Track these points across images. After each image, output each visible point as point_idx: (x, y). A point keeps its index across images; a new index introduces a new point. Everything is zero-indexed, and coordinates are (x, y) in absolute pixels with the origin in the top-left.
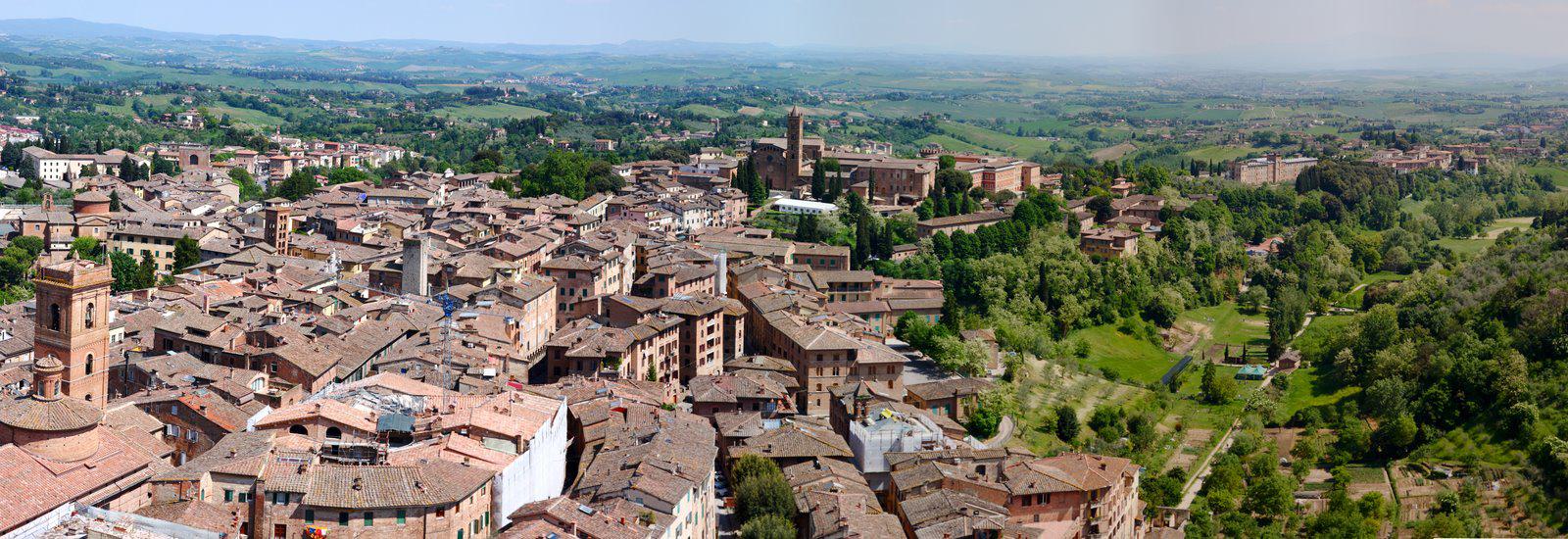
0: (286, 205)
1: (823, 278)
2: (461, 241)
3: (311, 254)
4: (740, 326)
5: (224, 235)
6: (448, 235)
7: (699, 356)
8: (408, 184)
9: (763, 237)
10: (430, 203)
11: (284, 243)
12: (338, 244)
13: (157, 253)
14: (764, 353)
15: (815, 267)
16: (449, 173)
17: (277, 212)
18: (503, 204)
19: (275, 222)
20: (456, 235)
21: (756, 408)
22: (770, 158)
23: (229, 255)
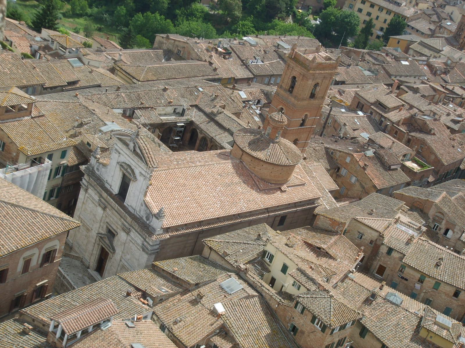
13: (377, 18)
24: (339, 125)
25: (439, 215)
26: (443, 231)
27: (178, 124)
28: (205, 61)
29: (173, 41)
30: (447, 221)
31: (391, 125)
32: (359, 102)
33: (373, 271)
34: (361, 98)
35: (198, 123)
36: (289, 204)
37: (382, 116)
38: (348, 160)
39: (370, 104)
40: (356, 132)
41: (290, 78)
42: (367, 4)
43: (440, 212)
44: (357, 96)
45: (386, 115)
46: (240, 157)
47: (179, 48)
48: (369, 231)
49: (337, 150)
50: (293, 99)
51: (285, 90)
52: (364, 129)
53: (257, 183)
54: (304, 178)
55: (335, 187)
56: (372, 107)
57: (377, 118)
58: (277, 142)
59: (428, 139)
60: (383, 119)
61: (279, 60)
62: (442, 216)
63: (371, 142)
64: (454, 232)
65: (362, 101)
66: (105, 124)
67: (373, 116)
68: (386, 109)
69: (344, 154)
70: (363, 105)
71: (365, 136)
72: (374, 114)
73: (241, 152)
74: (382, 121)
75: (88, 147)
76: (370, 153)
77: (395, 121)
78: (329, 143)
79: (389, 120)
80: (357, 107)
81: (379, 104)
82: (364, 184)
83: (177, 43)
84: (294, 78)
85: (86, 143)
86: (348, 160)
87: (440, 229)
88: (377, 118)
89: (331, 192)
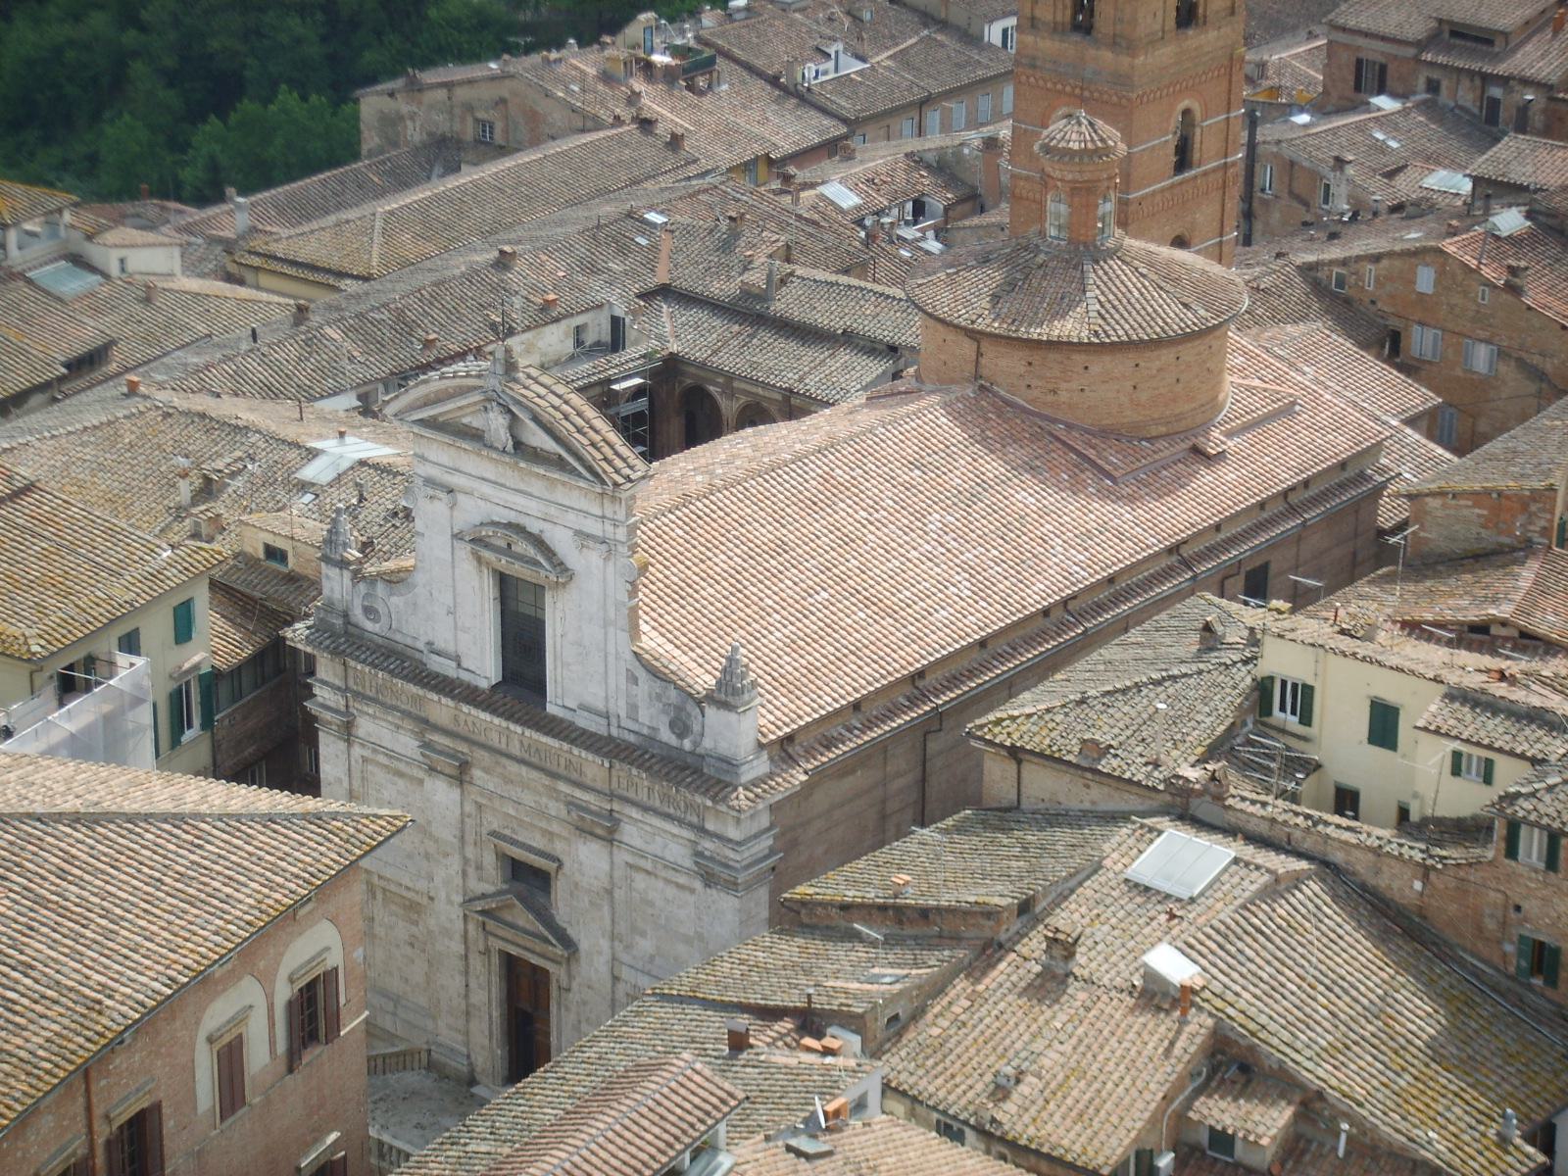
24: (1314, 176)
27: (616, 387)
28: (618, 121)
29: (441, 94)
31: (1542, 103)
32: (1359, 62)
34: (1361, 41)
35: (700, 355)
36: (1262, 505)
37: (1487, 79)
38: (1425, 280)
39: (1411, 52)
40: (1400, 181)
45: (1501, 69)
46: (970, 368)
47: (481, 115)
49: (1359, 258)
52: (1433, 160)
53: (1091, 453)
54: (1279, 380)
55: (1420, 397)
56: (1428, 57)
57: (1467, 96)
58: (1112, 253)
60: (1496, 92)
61: (926, 32)
63: (1491, 191)
65: (1374, 50)
66: (313, 454)
67: (1444, 98)
68: (1490, 42)
69: (1398, 263)
70: (1383, 68)
71: (1451, 182)
72: (1445, 84)
73: (968, 348)
74: (1494, 104)
75: (274, 565)
76: (1510, 220)
77: (1554, 79)
78: (1306, 250)
79: (1527, 82)
80: (1358, 88)
81: (1454, 34)
82: (1536, 360)
83: (462, 94)
85: (261, 554)
88: (1467, 96)
89: (1411, 422)
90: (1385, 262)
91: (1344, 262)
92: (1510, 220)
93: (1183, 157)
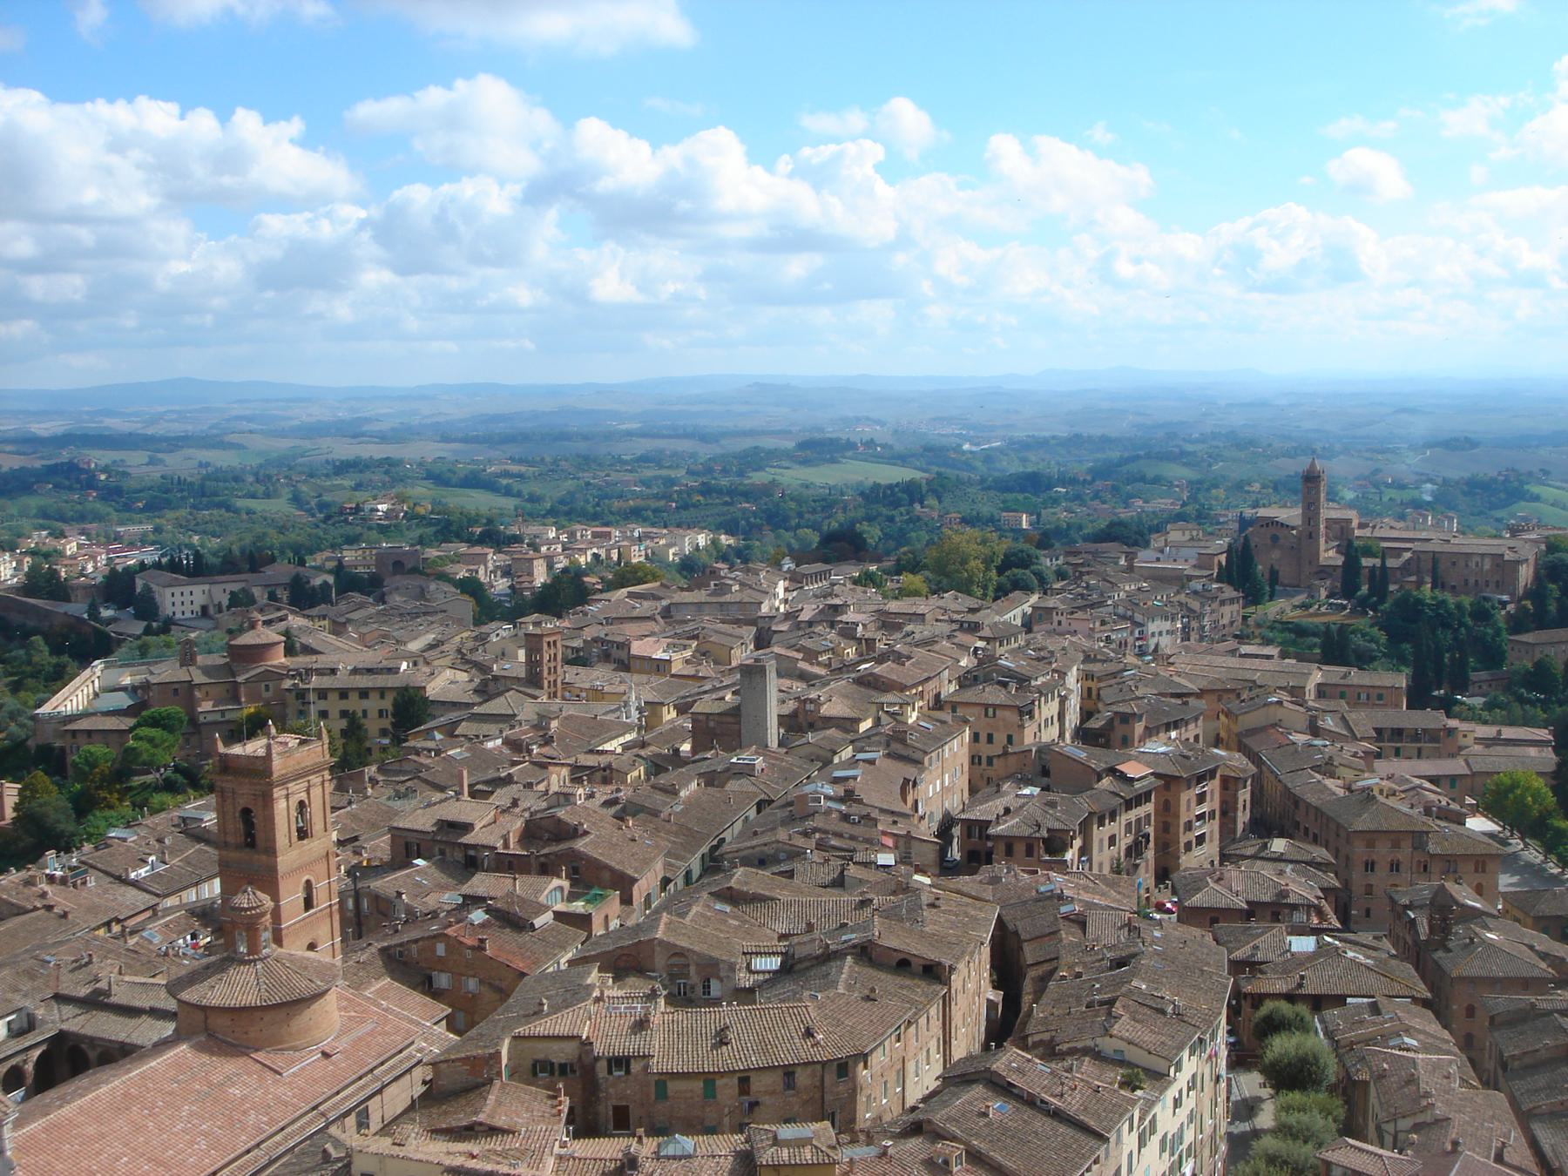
0: (550, 624)
1: (1364, 720)
2: (819, 664)
3: (597, 694)
4: (1244, 795)
5: (463, 677)
6: (800, 656)
7: (1183, 839)
8: (731, 582)
9: (1269, 657)
10: (765, 609)
11: (555, 681)
12: (636, 677)
13: (365, 712)
14: (1281, 836)
15: (1355, 703)
16: (788, 564)
17: (542, 636)
18: (876, 608)
19: (540, 651)
20: (811, 656)
21: (1276, 918)
22: (1275, 538)
23: (471, 705)
24: (388, 901)
25: (675, 960)
26: (699, 989)
30: (697, 965)
33: (607, 1129)
37: (467, 846)
38: (441, 949)
41: (237, 814)
42: (333, 697)
43: (675, 954)
44: (398, 833)
48: (555, 1046)
50: (264, 858)
51: (237, 847)
52: (443, 888)
59: (580, 845)
60: (472, 853)
61: (198, 847)
62: (681, 961)
64: (722, 981)
65: (412, 838)
71: (451, 898)
73: (200, 1016)
80: (407, 856)
82: (497, 983)
84: (246, 813)
86: (441, 949)
87: (693, 987)
90: (421, 943)
91: (401, 945)
92: (478, 916)
93: (308, 904)
